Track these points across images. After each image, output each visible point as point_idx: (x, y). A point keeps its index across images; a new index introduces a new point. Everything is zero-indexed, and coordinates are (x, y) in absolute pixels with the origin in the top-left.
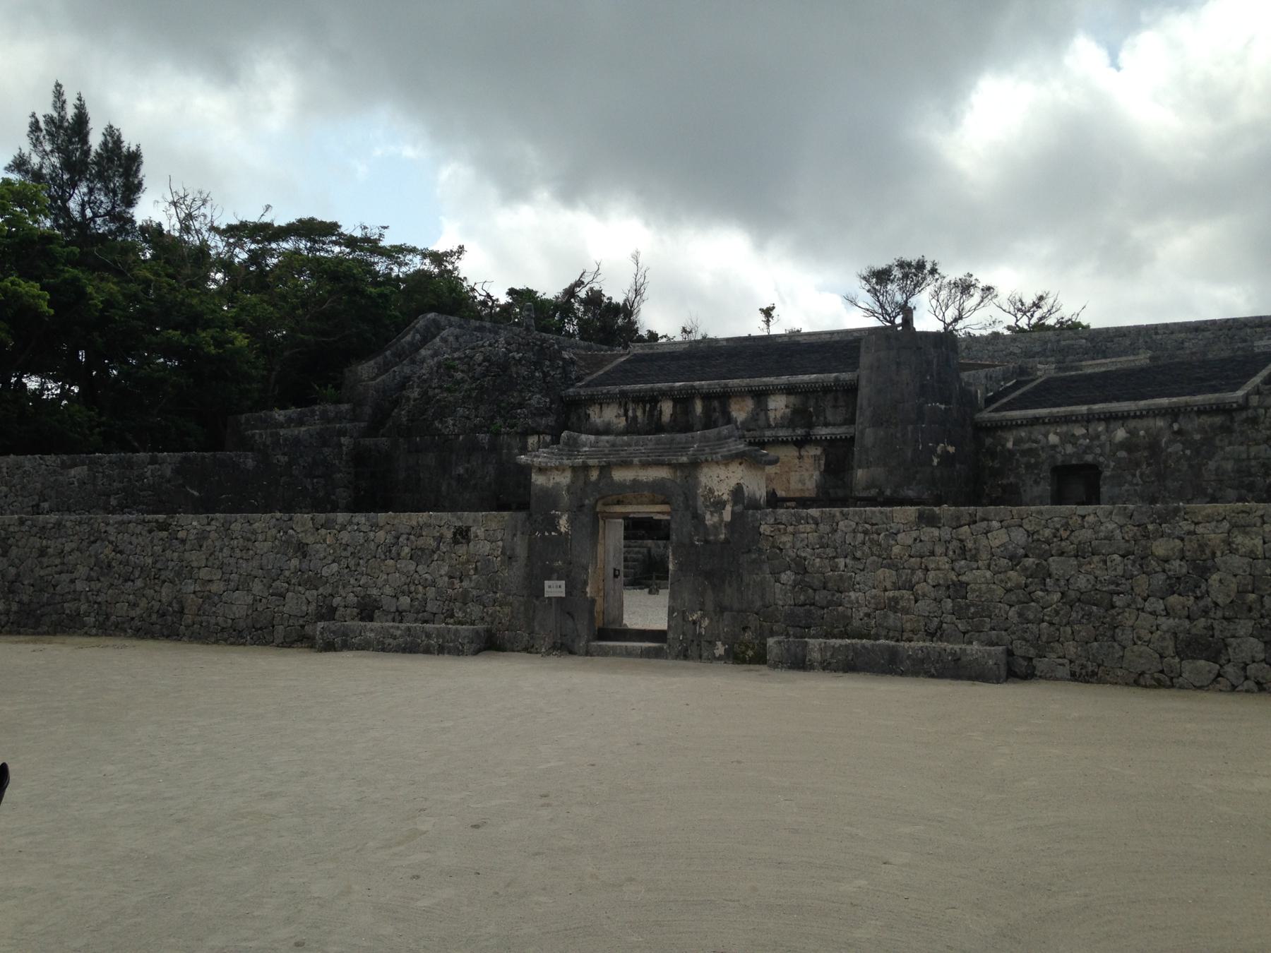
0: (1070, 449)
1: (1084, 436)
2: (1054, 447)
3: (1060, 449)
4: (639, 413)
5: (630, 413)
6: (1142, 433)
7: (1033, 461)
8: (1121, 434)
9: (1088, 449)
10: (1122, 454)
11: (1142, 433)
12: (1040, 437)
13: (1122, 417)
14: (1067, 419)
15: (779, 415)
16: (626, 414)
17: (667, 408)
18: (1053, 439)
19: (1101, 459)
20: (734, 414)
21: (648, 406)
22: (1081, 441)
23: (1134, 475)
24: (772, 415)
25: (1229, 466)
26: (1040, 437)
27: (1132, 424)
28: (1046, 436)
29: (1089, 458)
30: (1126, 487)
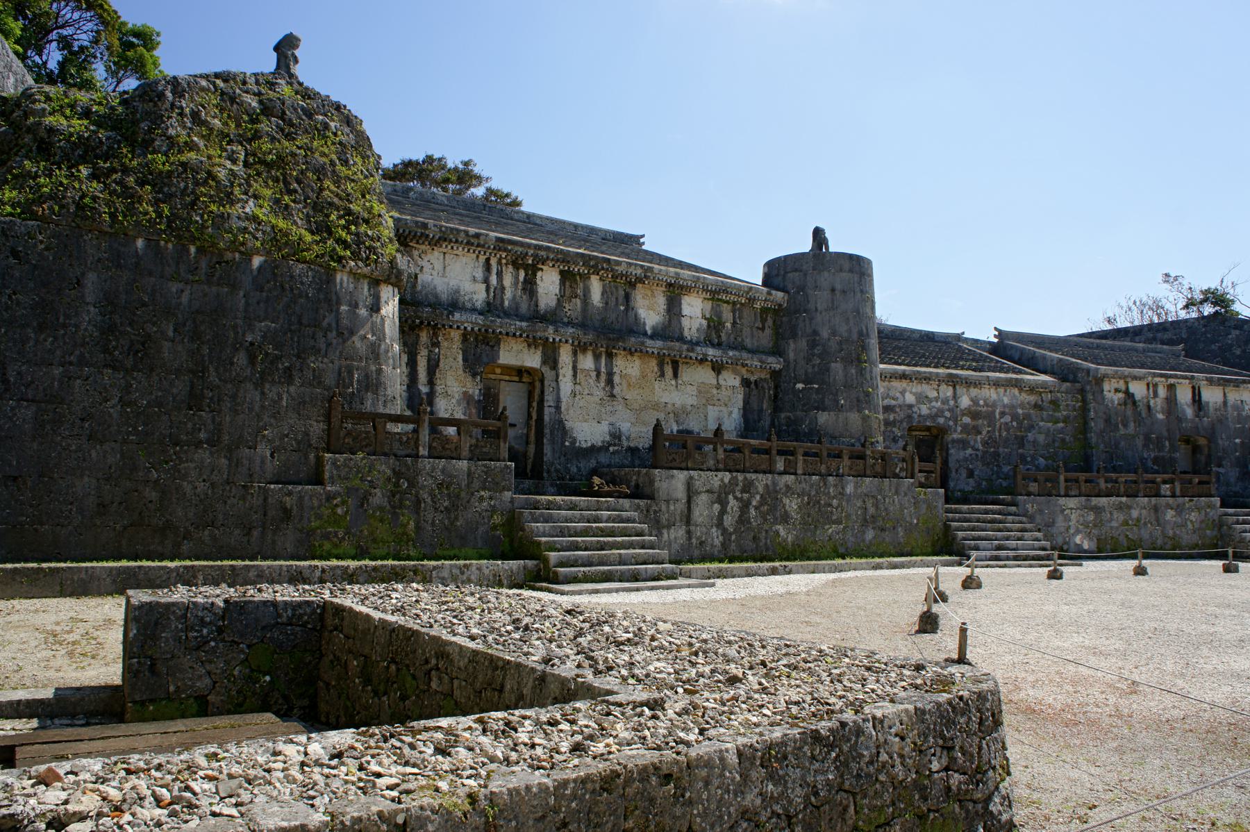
0: (924, 410)
1: (937, 399)
2: (910, 406)
3: (915, 409)
4: (508, 281)
5: (494, 279)
6: (981, 402)
7: (891, 418)
8: (965, 402)
9: (940, 413)
10: (966, 420)
11: (981, 402)
12: (898, 395)
13: (968, 383)
14: (927, 379)
15: (695, 325)
16: (486, 281)
17: (549, 283)
18: (910, 398)
19: (951, 423)
20: (642, 313)
21: (522, 274)
22: (934, 404)
23: (976, 441)
24: (685, 323)
25: (1041, 438)
26: (898, 395)
27: (974, 392)
28: (903, 393)
29: (941, 420)
30: (969, 451)
